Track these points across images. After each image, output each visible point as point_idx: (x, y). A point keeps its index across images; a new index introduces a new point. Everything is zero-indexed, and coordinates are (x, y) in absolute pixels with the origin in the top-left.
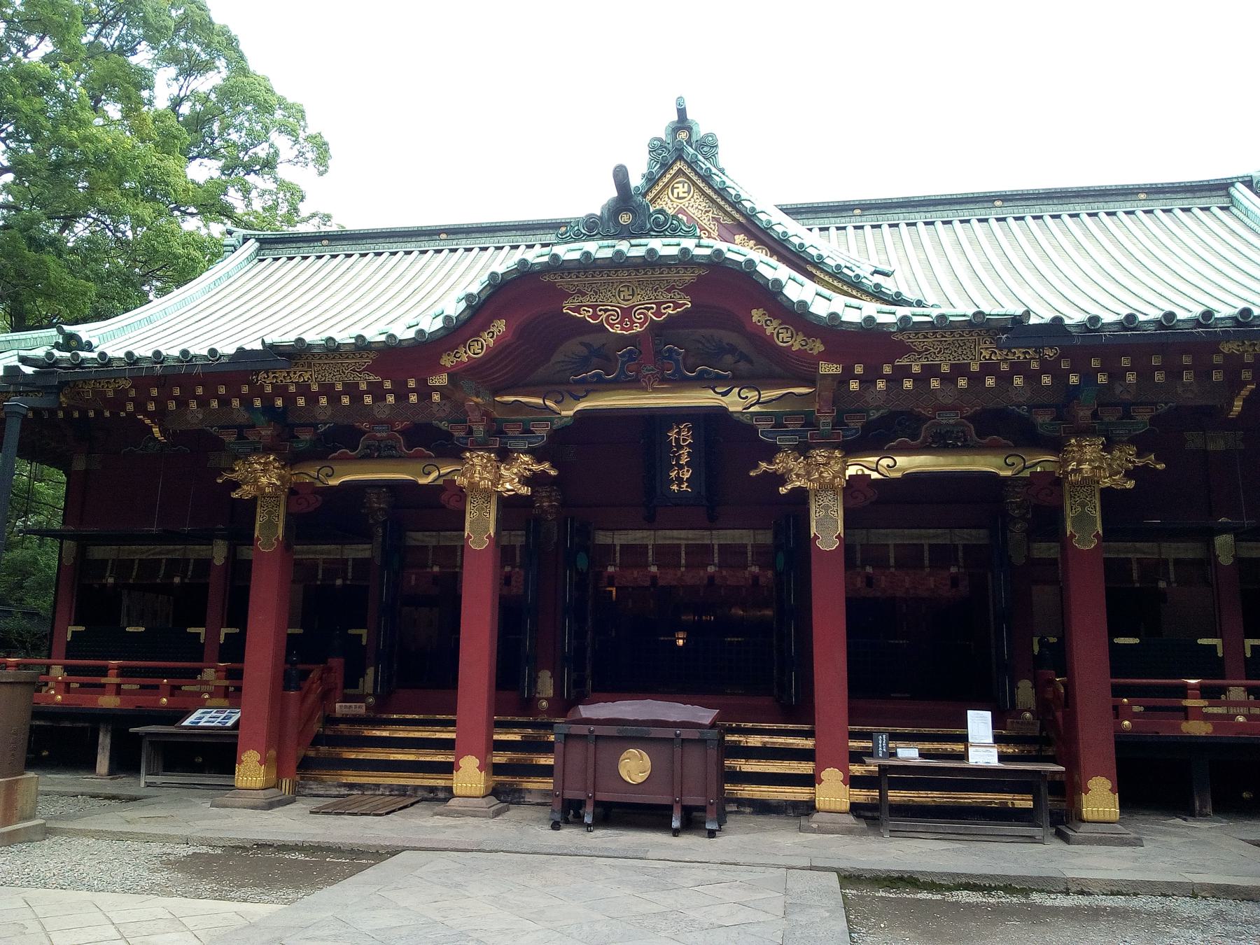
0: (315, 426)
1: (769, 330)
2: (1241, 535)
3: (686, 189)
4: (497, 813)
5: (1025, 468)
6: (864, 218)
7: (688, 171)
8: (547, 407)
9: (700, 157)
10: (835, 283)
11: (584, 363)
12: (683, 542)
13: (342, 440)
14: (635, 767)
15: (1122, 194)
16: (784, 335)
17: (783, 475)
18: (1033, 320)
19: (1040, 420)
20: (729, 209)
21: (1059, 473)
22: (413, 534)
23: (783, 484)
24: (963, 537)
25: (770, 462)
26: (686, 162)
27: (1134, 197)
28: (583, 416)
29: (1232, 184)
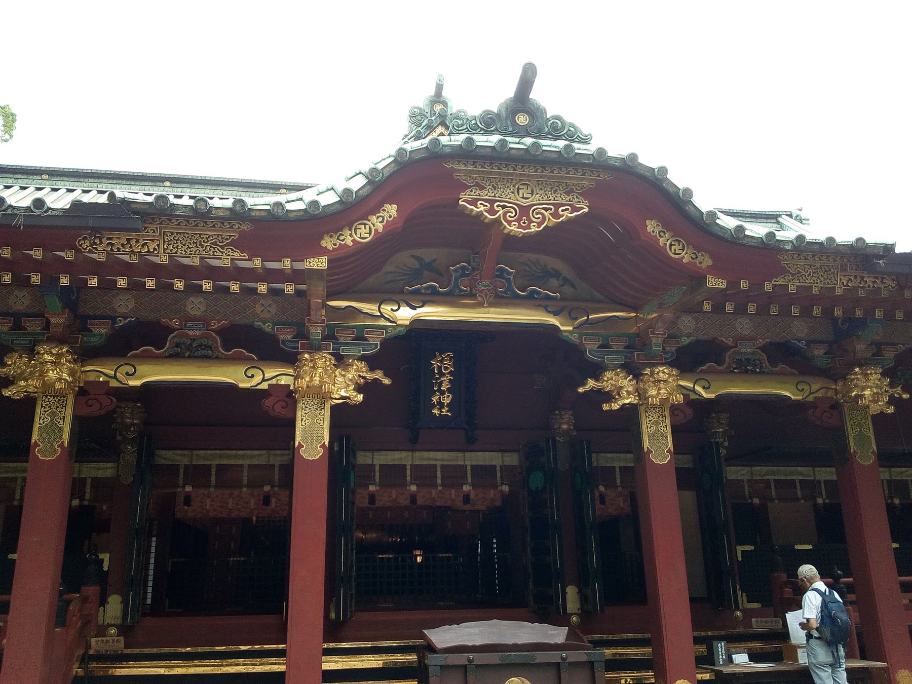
0: (113, 319)
1: (662, 241)
8: (382, 316)
11: (416, 275)
22: (163, 452)
25: (597, 380)
29: (780, 216)
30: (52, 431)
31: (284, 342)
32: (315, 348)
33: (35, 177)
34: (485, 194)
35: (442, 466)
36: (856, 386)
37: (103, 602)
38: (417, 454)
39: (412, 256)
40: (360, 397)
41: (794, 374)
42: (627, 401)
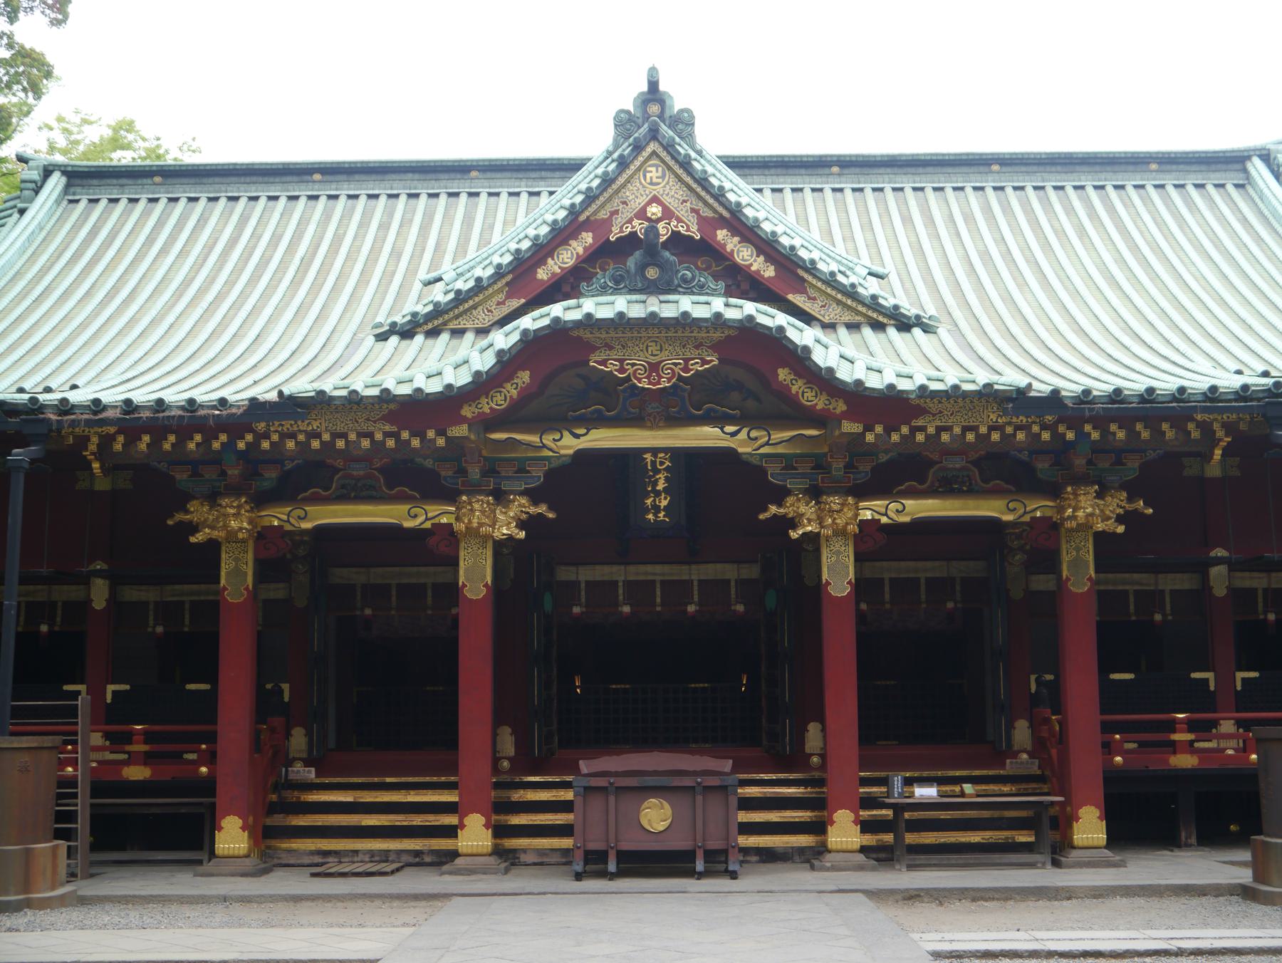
1: (794, 389)
2: (1233, 566)
3: (660, 174)
4: (507, 871)
5: (1025, 513)
6: (843, 179)
7: (663, 154)
8: (544, 446)
9: (677, 139)
10: (829, 290)
12: (658, 578)
13: (311, 476)
14: (656, 816)
15: (1134, 163)
16: (809, 394)
17: (793, 518)
18: (1033, 394)
19: (1040, 466)
20: (711, 201)
21: (1056, 518)
23: (794, 527)
24: (959, 569)
25: (780, 505)
26: (661, 144)
27: (1144, 167)
28: (581, 455)
29: (1249, 158)
30: (237, 575)
31: (445, 478)
32: (474, 490)
33: (145, 181)
34: (613, 354)
35: (662, 582)
36: (1070, 506)
37: (288, 735)
38: (632, 569)
39: (578, 375)
41: (1010, 492)
42: (809, 528)
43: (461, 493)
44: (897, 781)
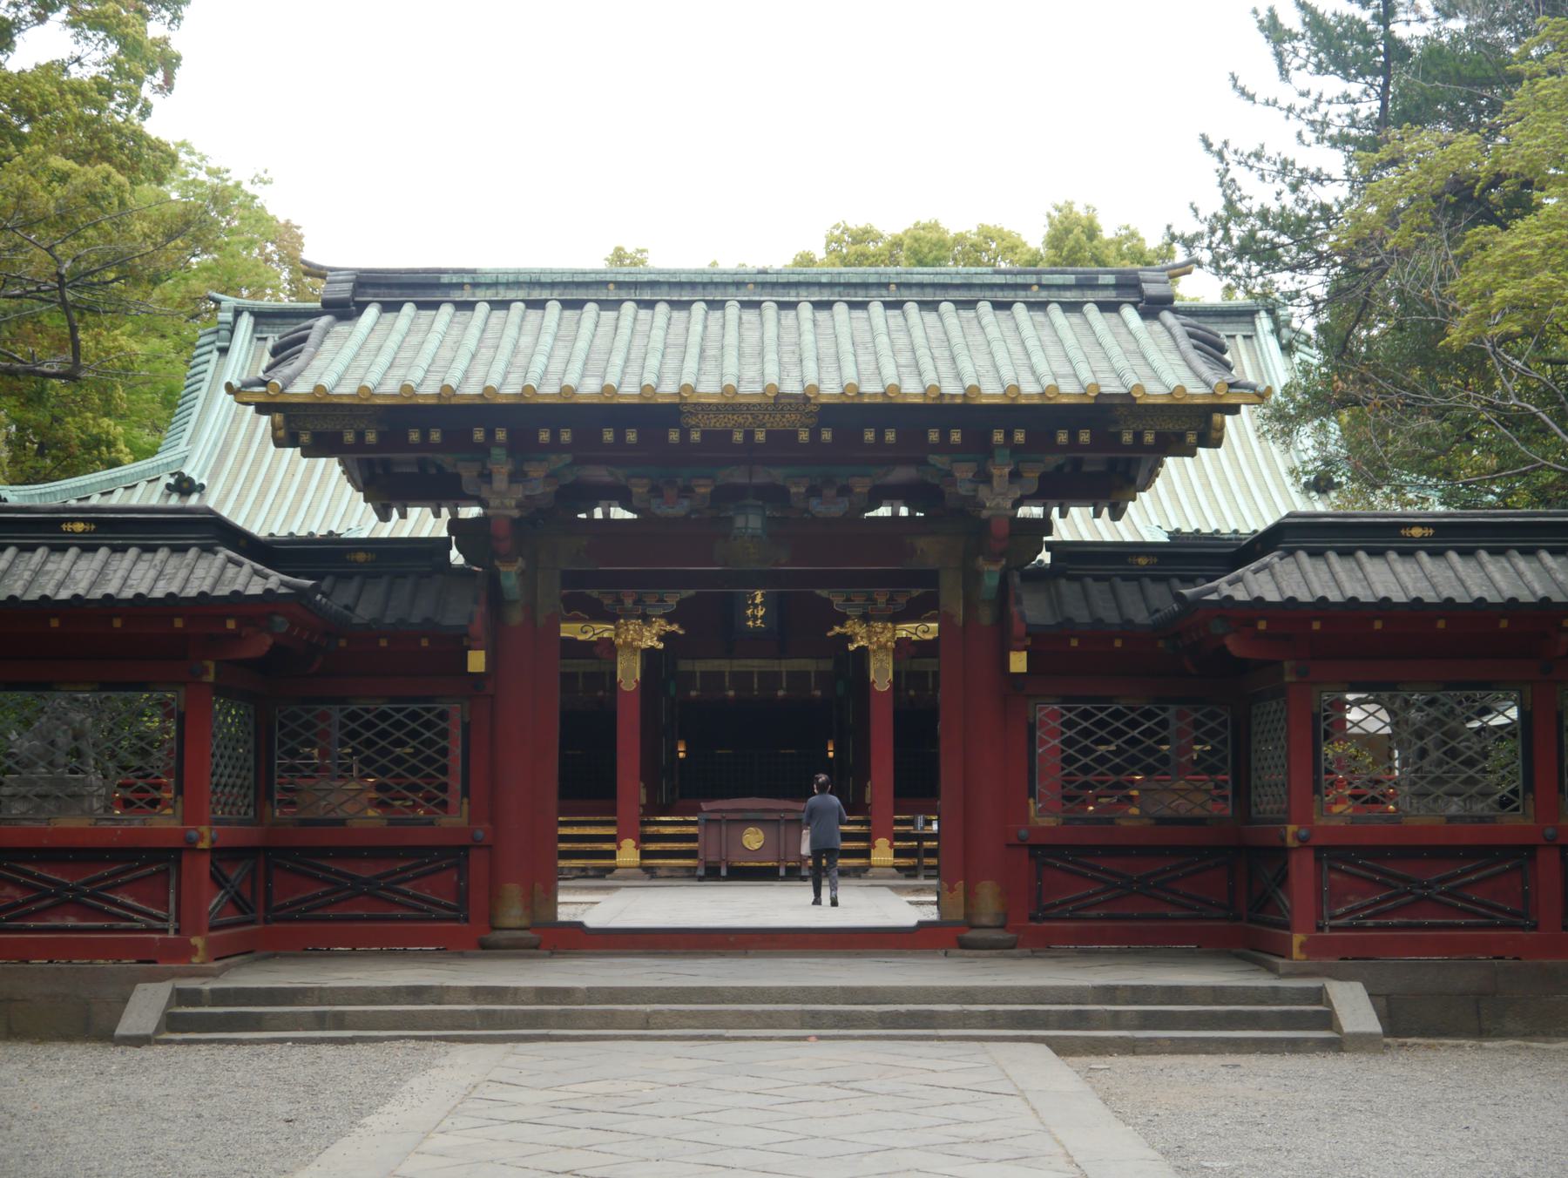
14: (753, 839)
25: (842, 626)
35: (760, 673)
38: (735, 662)
40: (661, 646)
43: (619, 617)
44: (920, 819)
